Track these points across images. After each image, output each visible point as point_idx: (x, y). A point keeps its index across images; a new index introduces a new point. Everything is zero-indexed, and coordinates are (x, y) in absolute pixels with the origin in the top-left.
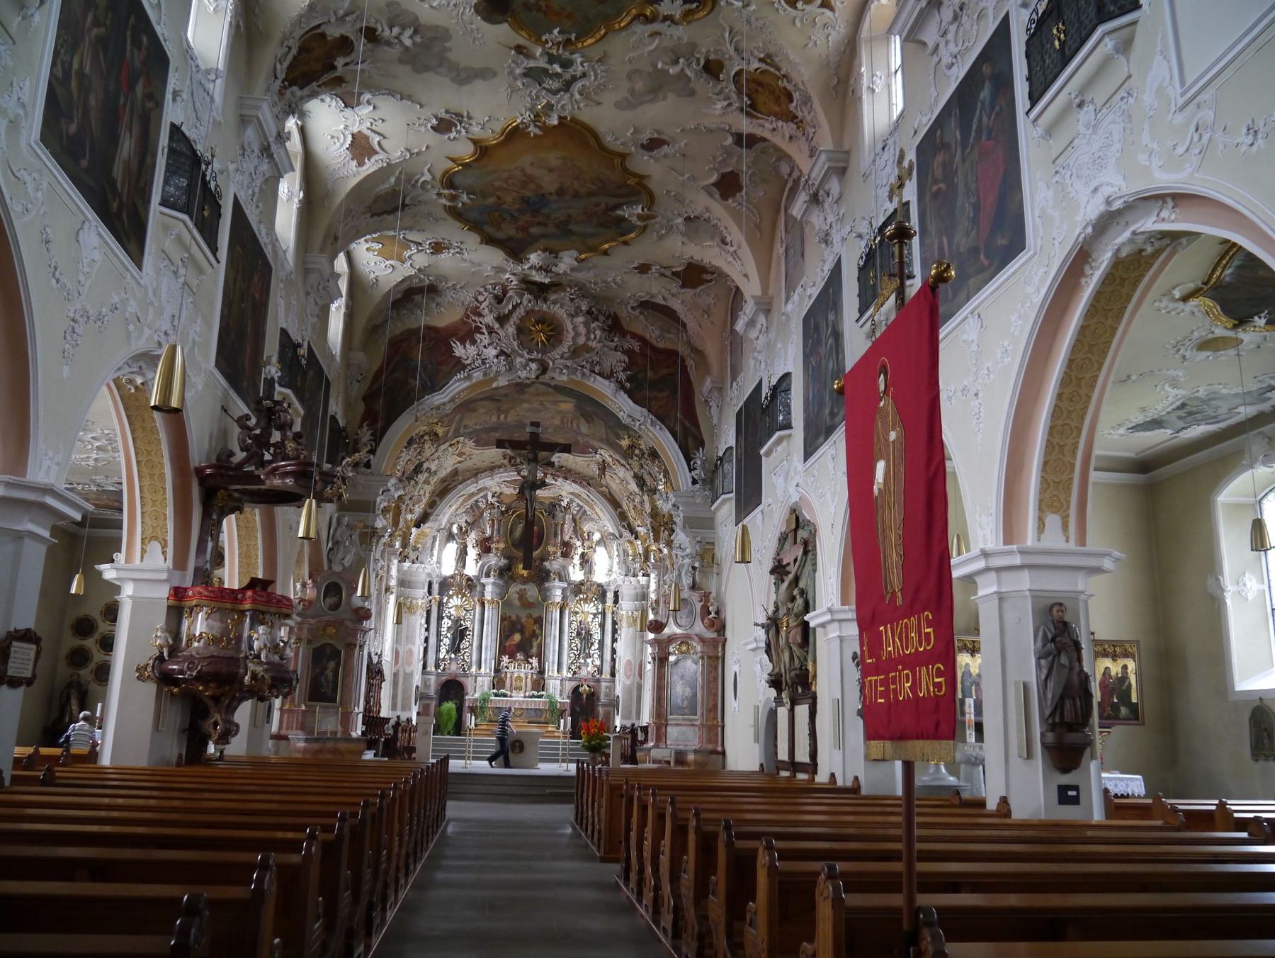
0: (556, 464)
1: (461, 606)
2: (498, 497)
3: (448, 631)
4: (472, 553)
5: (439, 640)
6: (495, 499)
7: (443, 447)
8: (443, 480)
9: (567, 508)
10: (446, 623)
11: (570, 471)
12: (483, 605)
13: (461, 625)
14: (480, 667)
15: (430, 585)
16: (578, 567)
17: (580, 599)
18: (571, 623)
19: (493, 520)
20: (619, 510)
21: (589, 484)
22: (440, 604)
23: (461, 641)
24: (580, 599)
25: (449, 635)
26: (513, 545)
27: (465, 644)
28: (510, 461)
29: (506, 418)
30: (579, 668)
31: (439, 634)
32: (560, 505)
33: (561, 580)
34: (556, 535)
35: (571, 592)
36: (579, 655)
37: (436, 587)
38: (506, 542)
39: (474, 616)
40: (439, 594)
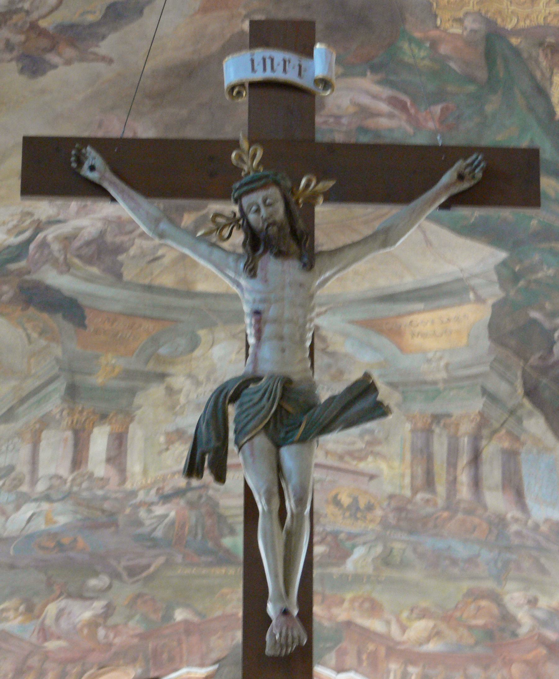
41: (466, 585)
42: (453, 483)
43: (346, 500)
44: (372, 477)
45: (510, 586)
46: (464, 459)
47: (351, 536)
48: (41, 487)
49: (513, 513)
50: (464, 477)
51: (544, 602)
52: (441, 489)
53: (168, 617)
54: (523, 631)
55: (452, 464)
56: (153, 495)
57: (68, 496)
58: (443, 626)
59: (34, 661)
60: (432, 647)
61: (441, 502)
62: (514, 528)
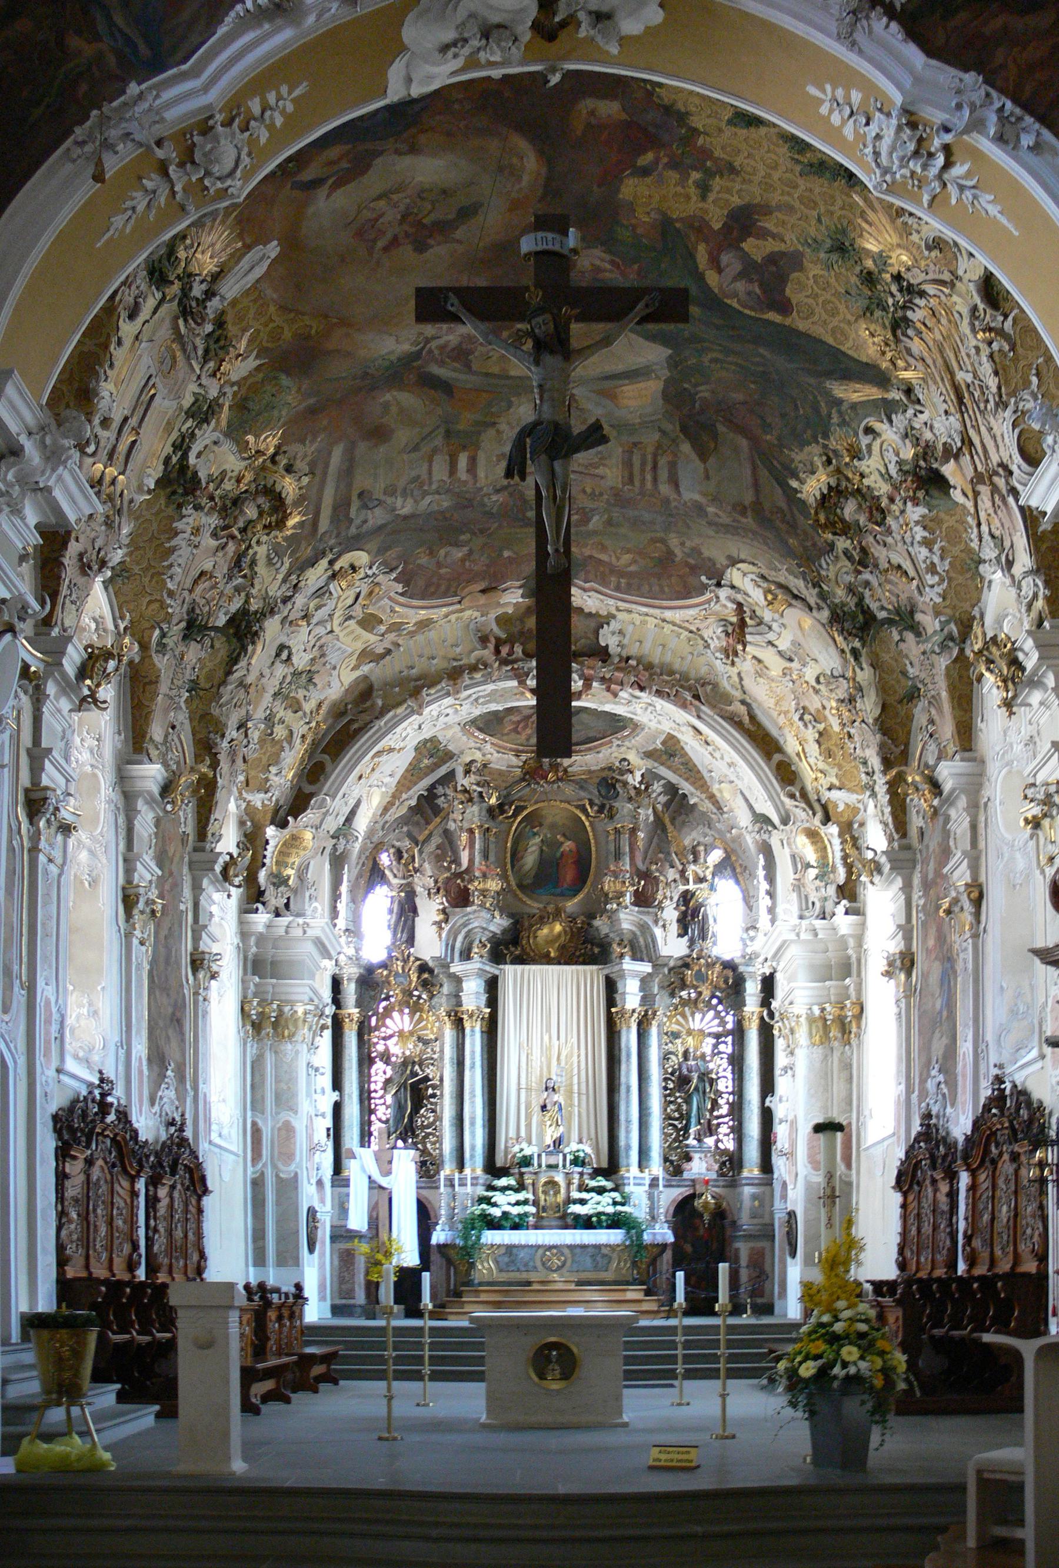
0: (613, 650)
1: (411, 1033)
2: (479, 772)
3: (384, 1088)
4: (429, 910)
5: (367, 1110)
6: (473, 778)
7: (315, 576)
8: (338, 711)
9: (641, 793)
10: (380, 1072)
11: (649, 667)
12: (459, 1024)
13: (414, 1074)
15: (336, 984)
19: (471, 831)
22: (364, 1030)
23: (416, 1109)
25: (389, 1099)
26: (520, 886)
27: (425, 1115)
28: (497, 652)
29: (472, 469)
31: (365, 1096)
32: (625, 784)
37: (350, 990)
38: (504, 877)
39: (442, 1051)
40: (359, 1004)
41: (649, 535)
42: (643, 481)
43: (589, 490)
44: (602, 477)
45: (672, 535)
46: (649, 467)
47: (592, 510)
48: (434, 487)
49: (673, 496)
50: (649, 477)
51: (688, 544)
52: (637, 483)
53: (500, 555)
54: (677, 559)
55: (643, 470)
56: (491, 490)
57: (448, 491)
58: (638, 558)
59: (435, 580)
60: (632, 568)
61: (637, 491)
62: (674, 504)
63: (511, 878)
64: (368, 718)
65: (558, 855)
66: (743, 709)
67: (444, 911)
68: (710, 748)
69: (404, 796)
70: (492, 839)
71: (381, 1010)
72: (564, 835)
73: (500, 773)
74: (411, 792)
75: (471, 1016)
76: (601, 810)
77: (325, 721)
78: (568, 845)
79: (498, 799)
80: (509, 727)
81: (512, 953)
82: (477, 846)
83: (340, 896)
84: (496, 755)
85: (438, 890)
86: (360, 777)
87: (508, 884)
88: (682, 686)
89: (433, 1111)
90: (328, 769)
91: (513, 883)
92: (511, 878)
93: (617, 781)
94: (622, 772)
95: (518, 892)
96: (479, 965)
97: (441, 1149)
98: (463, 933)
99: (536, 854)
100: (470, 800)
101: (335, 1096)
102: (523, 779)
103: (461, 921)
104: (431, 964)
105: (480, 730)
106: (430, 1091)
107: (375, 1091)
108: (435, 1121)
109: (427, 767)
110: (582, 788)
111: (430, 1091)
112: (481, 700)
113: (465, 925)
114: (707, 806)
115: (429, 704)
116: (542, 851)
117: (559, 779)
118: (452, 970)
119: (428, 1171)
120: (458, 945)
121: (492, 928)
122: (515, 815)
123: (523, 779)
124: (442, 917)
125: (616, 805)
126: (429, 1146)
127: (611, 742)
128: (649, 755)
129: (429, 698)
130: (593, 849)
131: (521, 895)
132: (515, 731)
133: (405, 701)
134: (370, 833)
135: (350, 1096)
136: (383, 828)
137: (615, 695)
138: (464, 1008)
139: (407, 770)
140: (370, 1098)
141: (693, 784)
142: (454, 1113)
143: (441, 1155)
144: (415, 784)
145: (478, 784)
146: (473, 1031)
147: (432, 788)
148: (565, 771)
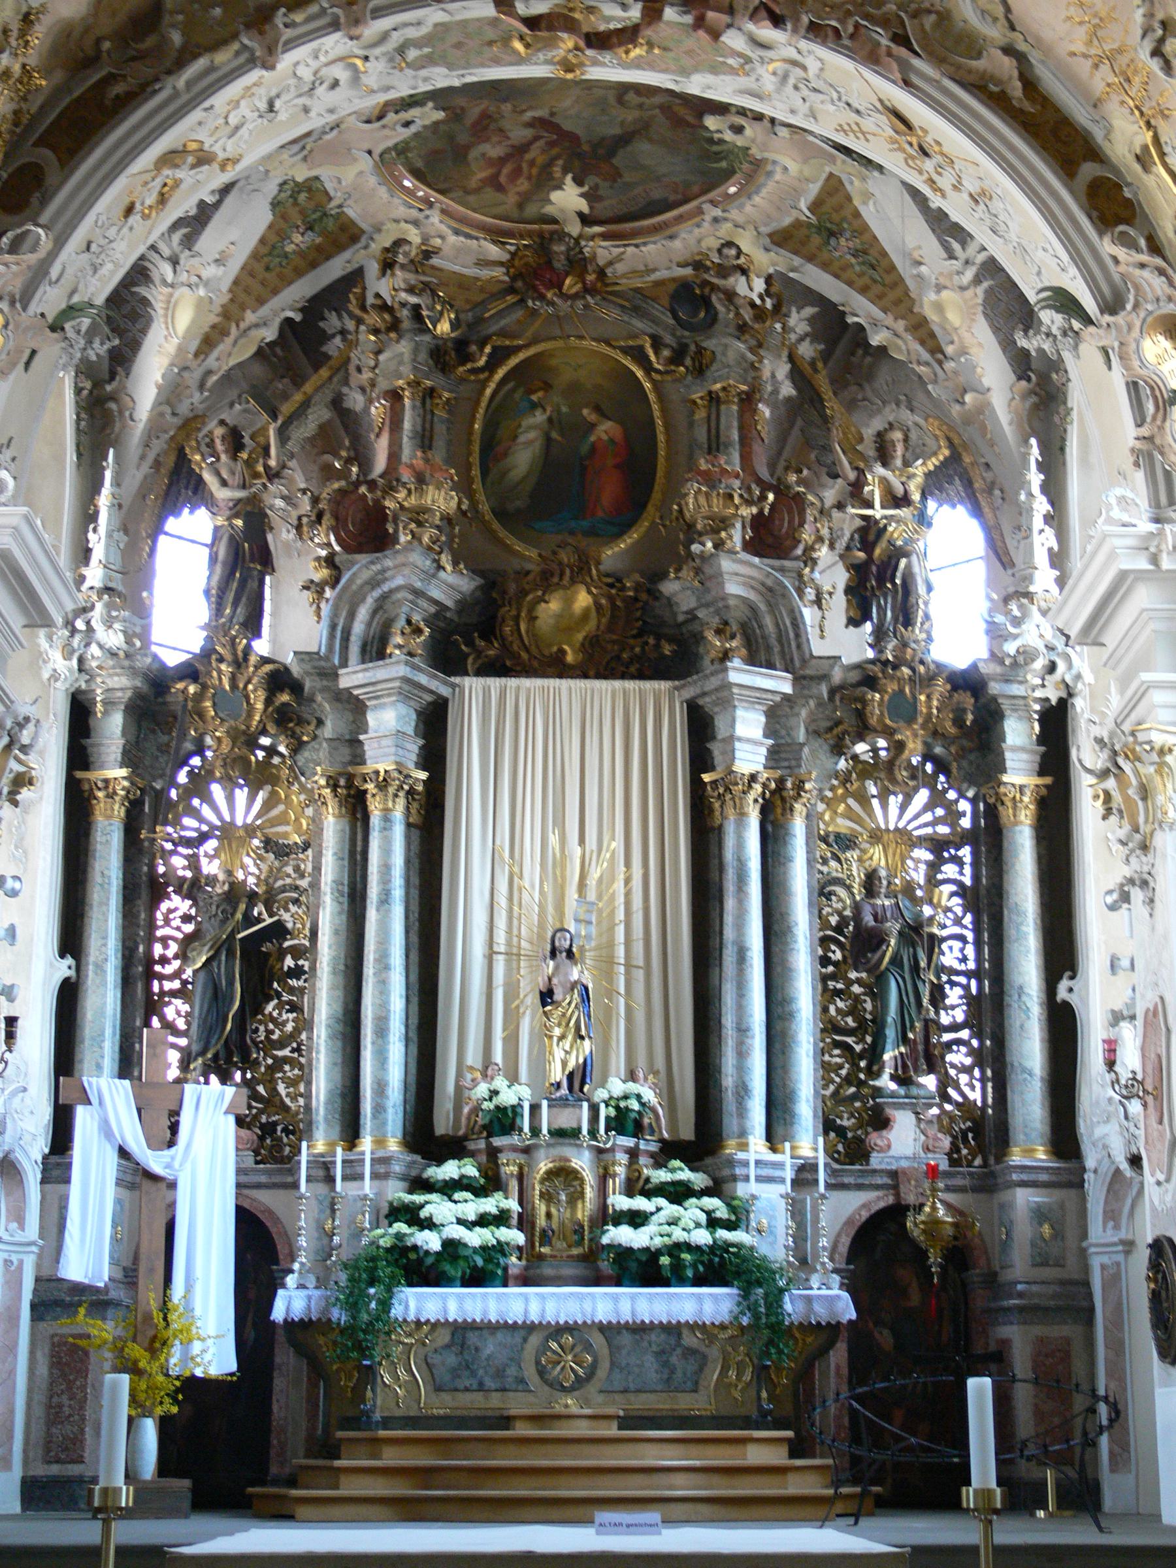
3: (183, 955)
6: (400, 277)
14: (351, 1132)
16: (838, 605)
17: (864, 770)
18: (822, 891)
19: (395, 396)
20: (1089, 170)
21: (901, 39)
24: (864, 770)
26: (500, 514)
30: (881, 1122)
32: (730, 296)
33: (757, 657)
34: (715, 446)
35: (814, 733)
36: (874, 1054)
38: (464, 487)
39: (317, 868)
40: (129, 758)
63: (481, 497)
64: (149, 72)
65: (584, 449)
66: (1007, 66)
67: (330, 561)
68: (929, 165)
69: (250, 317)
70: (440, 413)
71: (182, 777)
72: (598, 409)
73: (463, 283)
74: (265, 311)
75: (383, 785)
76: (677, 358)
77: (46, 72)
78: (606, 430)
79: (454, 325)
80: (481, 174)
81: (479, 653)
82: (407, 425)
83: (93, 518)
84: (452, 239)
85: (320, 516)
86: (129, 210)
87: (474, 504)
88: (867, 17)
89: (294, 1008)
90: (51, 179)
91: (485, 508)
92: (481, 497)
93: (714, 288)
94: (724, 271)
95: (496, 525)
96: (402, 670)
97: (308, 1096)
98: (370, 601)
99: (538, 446)
100: (394, 325)
101: (64, 968)
102: (511, 290)
103: (366, 575)
104: (296, 671)
105: (417, 174)
106: (289, 962)
107: (164, 960)
108: (297, 1031)
109: (301, 254)
110: (637, 311)
111: (289, 962)
112: (412, 54)
113: (374, 583)
114: (907, 348)
115: (291, 44)
116: (548, 440)
117: (588, 290)
118: (345, 682)
119: (278, 1145)
120: (358, 628)
121: (436, 594)
122: (491, 367)
123: (511, 290)
124: (324, 573)
125: (710, 344)
126: (281, 1088)
127: (700, 211)
128: (782, 239)
129: (288, 33)
130: (661, 438)
131: (502, 533)
132: (494, 183)
133: (235, 36)
134: (171, 394)
135: (101, 969)
136: (202, 386)
137: (716, 35)
138: (370, 767)
139: (255, 256)
140: (150, 975)
141: (877, 300)
142: (338, 1008)
143: (308, 1108)
144: (275, 292)
145: (411, 290)
146: (387, 819)
147: (315, 307)
148: (601, 273)
